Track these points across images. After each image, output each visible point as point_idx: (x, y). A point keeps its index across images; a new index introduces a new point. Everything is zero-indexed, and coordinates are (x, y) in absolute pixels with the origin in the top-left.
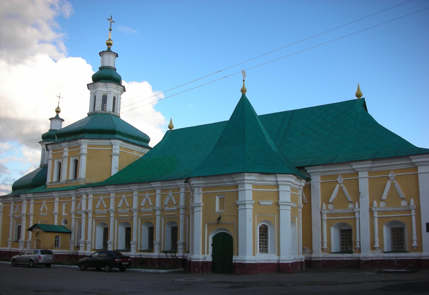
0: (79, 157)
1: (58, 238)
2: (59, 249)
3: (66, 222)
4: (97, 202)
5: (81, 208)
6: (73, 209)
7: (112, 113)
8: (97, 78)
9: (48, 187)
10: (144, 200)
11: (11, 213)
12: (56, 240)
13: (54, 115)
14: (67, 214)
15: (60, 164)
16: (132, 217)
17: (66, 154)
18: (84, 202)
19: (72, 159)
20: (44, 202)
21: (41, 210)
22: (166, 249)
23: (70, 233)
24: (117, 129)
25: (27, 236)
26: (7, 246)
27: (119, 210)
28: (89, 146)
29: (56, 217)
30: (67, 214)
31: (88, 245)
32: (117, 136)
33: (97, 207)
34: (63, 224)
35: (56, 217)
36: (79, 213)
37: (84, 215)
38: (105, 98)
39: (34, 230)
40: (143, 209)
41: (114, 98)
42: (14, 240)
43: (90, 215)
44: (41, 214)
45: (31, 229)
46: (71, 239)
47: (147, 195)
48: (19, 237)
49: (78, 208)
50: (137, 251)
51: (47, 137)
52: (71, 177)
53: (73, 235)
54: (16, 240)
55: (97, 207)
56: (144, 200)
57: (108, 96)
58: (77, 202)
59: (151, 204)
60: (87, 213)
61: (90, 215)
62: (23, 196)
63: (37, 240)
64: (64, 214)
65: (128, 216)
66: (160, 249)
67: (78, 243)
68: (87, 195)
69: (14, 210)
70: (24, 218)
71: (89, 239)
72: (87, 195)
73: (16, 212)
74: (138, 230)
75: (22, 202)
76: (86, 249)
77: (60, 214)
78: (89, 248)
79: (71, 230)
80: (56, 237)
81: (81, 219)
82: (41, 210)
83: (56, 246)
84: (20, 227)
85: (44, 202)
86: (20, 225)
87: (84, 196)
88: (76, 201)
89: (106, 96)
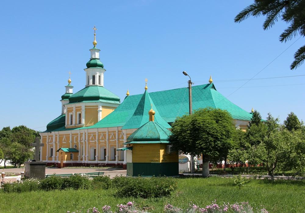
0: (81, 112)
1: (72, 155)
2: (73, 160)
3: (76, 146)
4: (90, 136)
5: (83, 140)
6: (79, 139)
7: (99, 85)
8: (89, 65)
9: (66, 128)
10: (111, 136)
11: (47, 142)
12: (71, 156)
13: (67, 84)
14: (76, 142)
15: (72, 116)
16: (106, 144)
17: (74, 110)
18: (84, 136)
19: (78, 113)
20: (64, 136)
21: (63, 140)
22: (121, 160)
23: (78, 152)
24: (101, 95)
25: (56, 155)
26: (46, 160)
27: (101, 141)
28: (85, 106)
29: (71, 144)
30: (76, 142)
31: (87, 158)
32: (100, 100)
33: (90, 139)
34: (75, 148)
35: (71, 144)
36: (82, 142)
37: (84, 143)
38: (94, 78)
39: (59, 151)
40: (111, 141)
41: (99, 76)
42: (49, 156)
43: (87, 143)
44: (63, 142)
45: (58, 151)
46: (78, 155)
47: (112, 133)
48: (52, 155)
49: (82, 139)
50: (109, 160)
51: (64, 97)
52: (78, 122)
53: (79, 153)
54: (51, 156)
55: (90, 139)
56: (111, 136)
57: (96, 75)
58: (81, 137)
59: (114, 138)
60: (85, 142)
61: (87, 143)
62: (53, 133)
63: (62, 156)
64: (75, 142)
65: (104, 143)
66: (118, 159)
67: (82, 157)
68: (85, 133)
69: (49, 140)
70: (54, 144)
71: (87, 155)
72: (85, 133)
73: (49, 141)
74: (109, 150)
75: (52, 136)
76: (85, 160)
77: (72, 142)
78: (87, 159)
79: (78, 151)
80: (71, 155)
81: (83, 145)
82: (63, 140)
83: (71, 159)
84: (52, 149)
85: (64, 136)
86: (52, 148)
87: (84, 133)
88: (81, 136)
89: (95, 76)
